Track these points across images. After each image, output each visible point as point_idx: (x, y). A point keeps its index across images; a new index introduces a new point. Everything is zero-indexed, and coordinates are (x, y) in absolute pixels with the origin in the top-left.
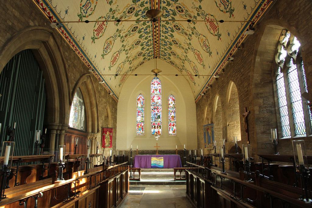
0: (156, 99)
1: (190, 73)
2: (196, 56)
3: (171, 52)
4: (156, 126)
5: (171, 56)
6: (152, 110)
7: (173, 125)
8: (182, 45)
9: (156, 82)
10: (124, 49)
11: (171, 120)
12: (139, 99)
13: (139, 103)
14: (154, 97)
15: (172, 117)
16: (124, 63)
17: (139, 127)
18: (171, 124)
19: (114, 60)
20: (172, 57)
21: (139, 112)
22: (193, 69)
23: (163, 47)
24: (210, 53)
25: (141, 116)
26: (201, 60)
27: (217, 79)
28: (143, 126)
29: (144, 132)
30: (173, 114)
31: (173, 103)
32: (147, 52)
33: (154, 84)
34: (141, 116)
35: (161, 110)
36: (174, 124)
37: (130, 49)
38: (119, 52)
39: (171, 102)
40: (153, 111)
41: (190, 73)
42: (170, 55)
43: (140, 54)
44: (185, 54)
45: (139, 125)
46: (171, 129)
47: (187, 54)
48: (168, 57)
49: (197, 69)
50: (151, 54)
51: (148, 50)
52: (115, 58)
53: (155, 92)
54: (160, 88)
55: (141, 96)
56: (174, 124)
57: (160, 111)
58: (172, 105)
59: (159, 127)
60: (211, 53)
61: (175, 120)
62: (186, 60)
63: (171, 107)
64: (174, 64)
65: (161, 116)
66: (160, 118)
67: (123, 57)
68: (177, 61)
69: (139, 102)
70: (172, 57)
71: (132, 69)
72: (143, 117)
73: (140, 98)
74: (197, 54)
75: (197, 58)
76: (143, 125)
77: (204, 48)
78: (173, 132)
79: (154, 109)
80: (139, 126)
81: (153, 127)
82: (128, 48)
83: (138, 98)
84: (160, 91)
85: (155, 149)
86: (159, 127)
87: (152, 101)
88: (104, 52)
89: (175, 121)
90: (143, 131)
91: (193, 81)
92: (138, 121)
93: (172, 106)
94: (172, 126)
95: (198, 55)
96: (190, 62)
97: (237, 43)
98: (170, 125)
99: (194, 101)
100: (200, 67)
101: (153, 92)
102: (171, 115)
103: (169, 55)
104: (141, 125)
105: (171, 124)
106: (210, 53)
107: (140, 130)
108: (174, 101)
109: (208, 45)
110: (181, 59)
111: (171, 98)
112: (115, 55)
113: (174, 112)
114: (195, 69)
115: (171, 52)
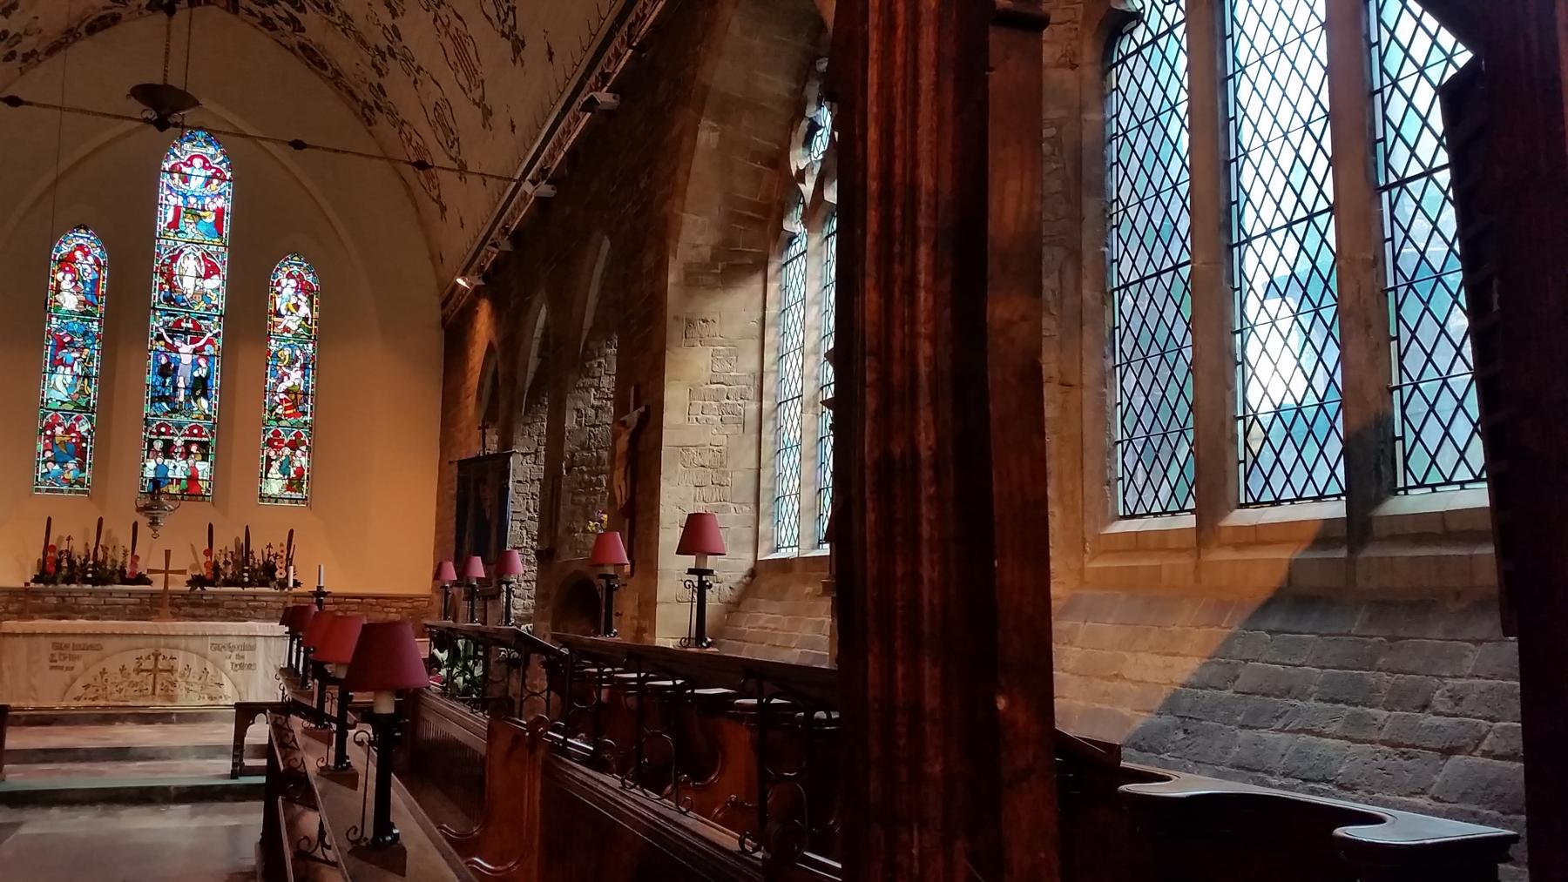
0: (189, 266)
1: (415, 137)
4: (179, 441)
6: (160, 337)
7: (294, 446)
9: (198, 162)
11: (279, 410)
12: (70, 258)
13: (66, 285)
14: (174, 259)
17: (57, 440)
18: (276, 433)
21: (61, 345)
22: (431, 116)
24: (518, 46)
26: (472, 73)
27: (541, 202)
28: (84, 439)
30: (295, 378)
31: (304, 310)
33: (186, 179)
34: (77, 369)
35: (219, 342)
36: (298, 435)
39: (290, 303)
40: (160, 346)
41: (415, 137)
45: (59, 430)
46: (276, 465)
47: (398, 22)
48: (284, 15)
49: (451, 124)
53: (190, 230)
54: (220, 202)
55: (82, 238)
56: (298, 435)
57: (209, 350)
58: (292, 322)
60: (523, 44)
61: (305, 414)
62: (393, 55)
63: (286, 329)
64: (324, 67)
65: (215, 383)
66: (205, 395)
68: (344, 55)
69: (69, 277)
71: (20, 49)
72: (87, 376)
73: (78, 254)
74: (452, 31)
75: (452, 58)
78: (289, 488)
79: (171, 337)
80: (53, 436)
81: (158, 445)
83: (65, 249)
84: (218, 224)
86: (194, 448)
87: (158, 279)
89: (308, 418)
90: (82, 469)
91: (435, 193)
92: (52, 405)
93: (294, 327)
94: (287, 451)
95: (459, 41)
96: (416, 71)
97: (632, 18)
98: (270, 443)
99: (438, 314)
100: (466, 116)
101: (174, 224)
102: (287, 384)
105: (276, 433)
106: (518, 46)
107: (62, 464)
108: (311, 298)
110: (364, 43)
111: (290, 276)
114: (441, 116)
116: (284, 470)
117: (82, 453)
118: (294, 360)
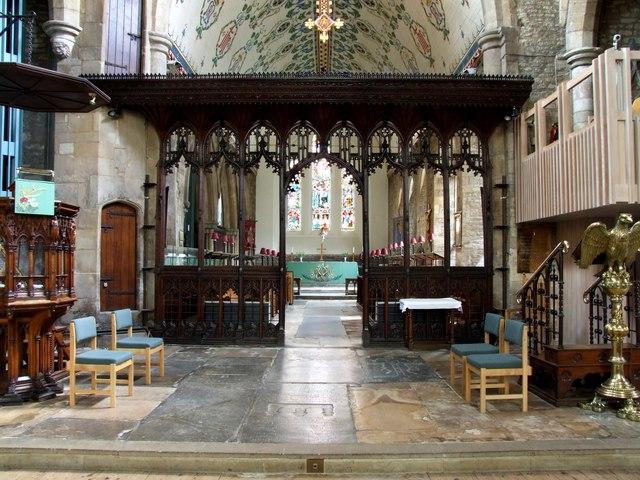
2: (416, 36)
3: (358, 24)
5: (356, 31)
8: (384, 9)
10: (248, 16)
16: (247, 48)
19: (226, 42)
20: (360, 35)
23: (340, 11)
32: (299, 21)
37: (261, 15)
38: (236, 24)
42: (352, 51)
43: (283, 28)
44: (391, 30)
50: (309, 47)
51: (304, 39)
52: (228, 38)
67: (244, 33)
70: (360, 35)
77: (434, 20)
82: (257, 13)
88: (203, 22)
103: (353, 30)
109: (441, 12)
112: (227, 29)
115: (358, 24)
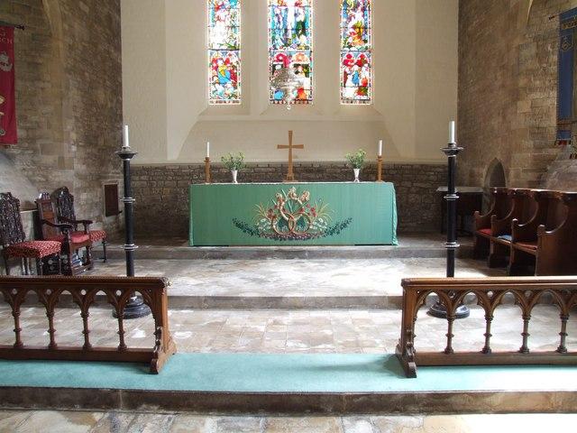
7: (360, 64)
15: (354, 27)
17: (220, 69)
18: (349, 56)
25: (228, 23)
28: (234, 67)
29: (239, 90)
30: (358, 18)
36: (362, 57)
45: (220, 63)
46: (350, 77)
56: (362, 57)
59: (300, 69)
61: (365, 41)
65: (310, 27)
72: (233, 27)
76: (234, 60)
78: (359, 93)
85: (280, 157)
90: (235, 87)
94: (356, 68)
98: (346, 63)
102: (353, 22)
104: (227, 62)
105: (349, 56)
113: (364, 10)
116: (355, 81)
117: (234, 77)
118: (357, 6)
